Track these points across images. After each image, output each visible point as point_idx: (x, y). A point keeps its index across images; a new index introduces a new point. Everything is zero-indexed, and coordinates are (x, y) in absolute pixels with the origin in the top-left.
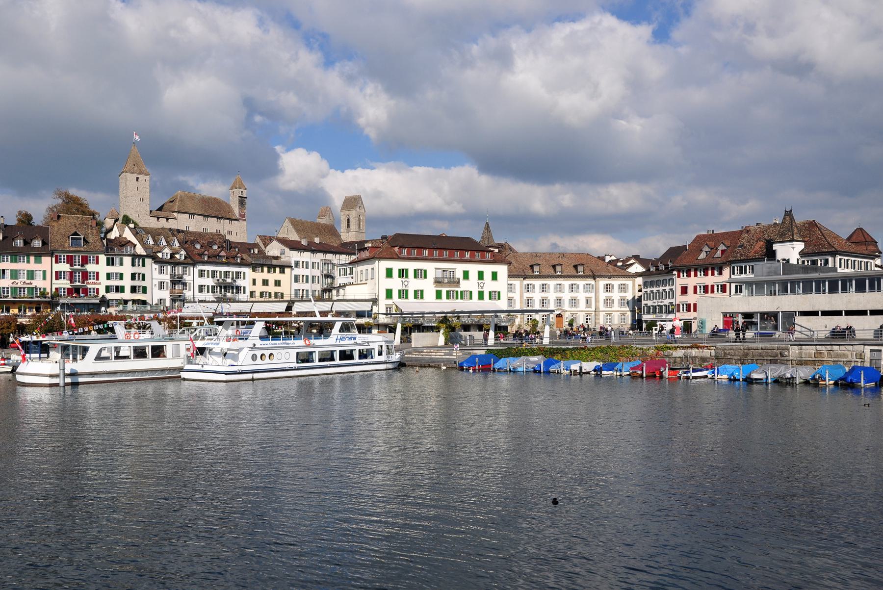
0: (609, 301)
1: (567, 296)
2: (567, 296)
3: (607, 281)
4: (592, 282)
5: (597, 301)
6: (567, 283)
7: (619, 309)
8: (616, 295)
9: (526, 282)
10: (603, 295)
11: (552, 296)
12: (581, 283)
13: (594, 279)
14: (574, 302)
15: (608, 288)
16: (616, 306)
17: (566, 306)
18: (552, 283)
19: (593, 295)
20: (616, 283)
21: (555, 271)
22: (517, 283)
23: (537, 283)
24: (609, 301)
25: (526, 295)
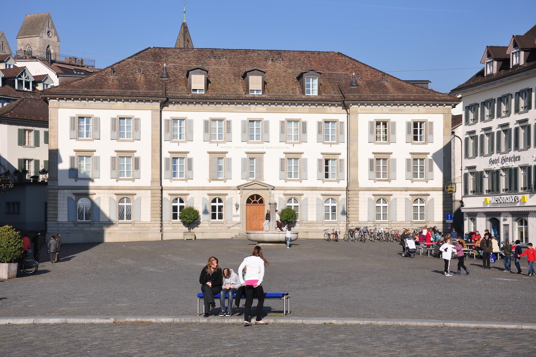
0: (380, 164)
1: (274, 151)
2: (274, 151)
3: (381, 113)
4: (337, 114)
5: (352, 162)
6: (274, 117)
7: (409, 184)
8: (401, 149)
9: (169, 113)
10: (366, 150)
11: (236, 149)
12: (312, 117)
13: (346, 107)
14: (291, 163)
15: (382, 130)
16: (401, 178)
17: (271, 175)
18: (237, 116)
19: (341, 149)
20: (401, 117)
21: (247, 90)
22: (144, 114)
23: (197, 116)
24: (380, 164)
25: (168, 147)
